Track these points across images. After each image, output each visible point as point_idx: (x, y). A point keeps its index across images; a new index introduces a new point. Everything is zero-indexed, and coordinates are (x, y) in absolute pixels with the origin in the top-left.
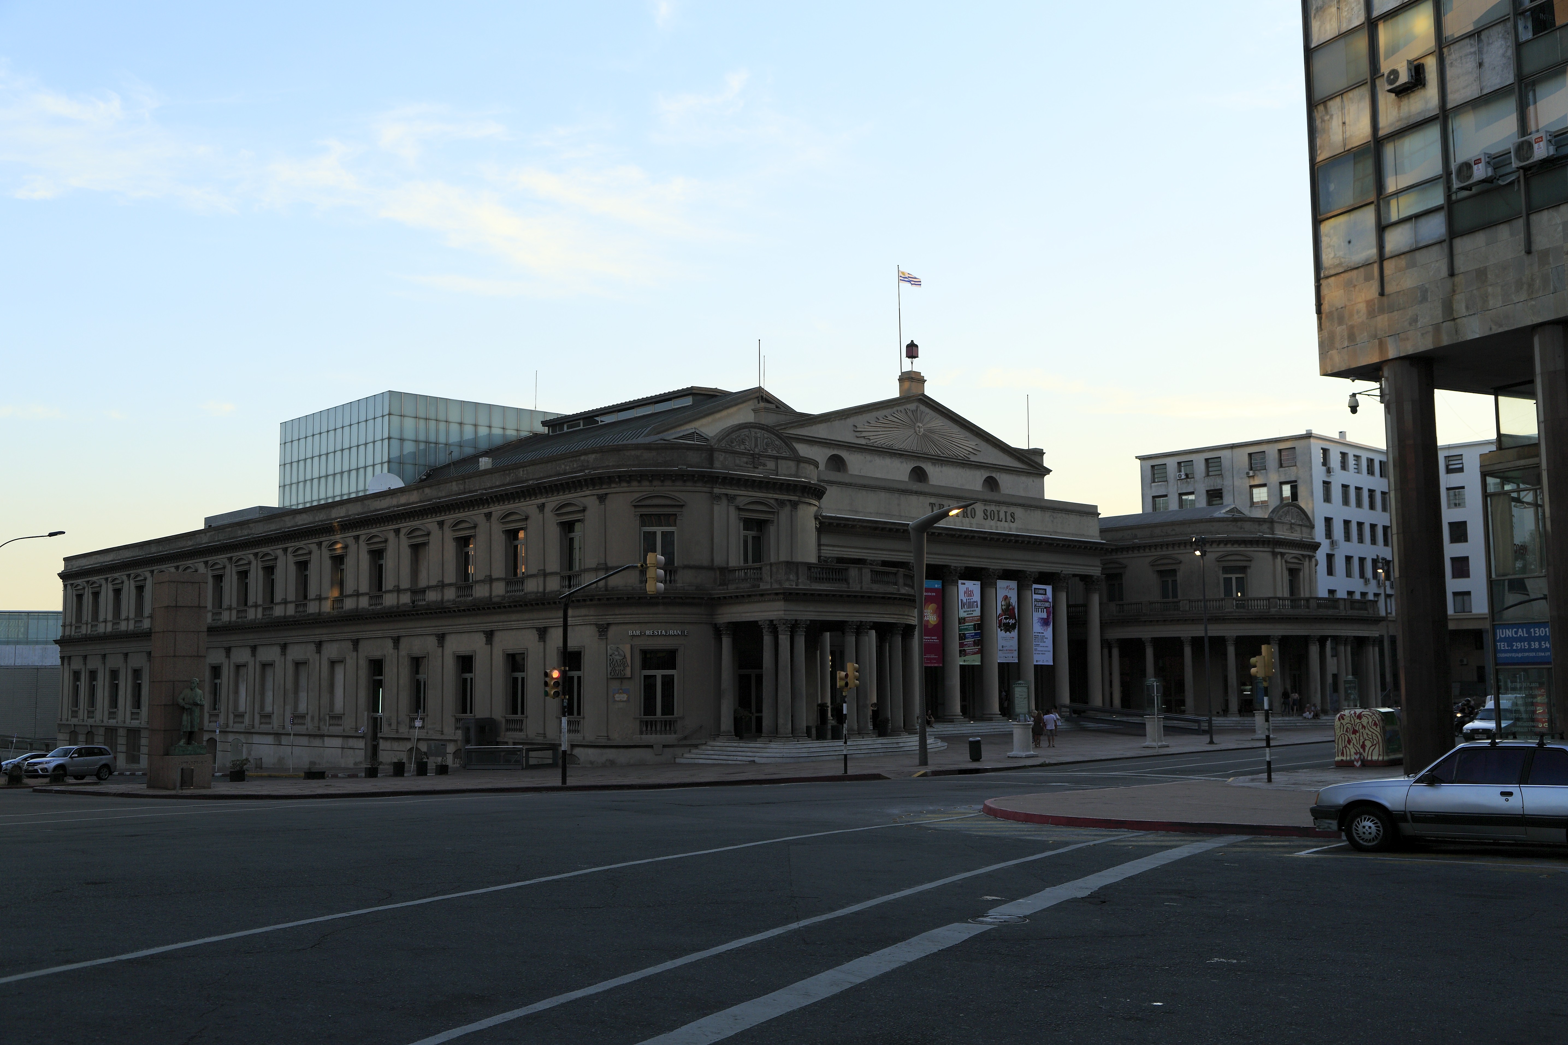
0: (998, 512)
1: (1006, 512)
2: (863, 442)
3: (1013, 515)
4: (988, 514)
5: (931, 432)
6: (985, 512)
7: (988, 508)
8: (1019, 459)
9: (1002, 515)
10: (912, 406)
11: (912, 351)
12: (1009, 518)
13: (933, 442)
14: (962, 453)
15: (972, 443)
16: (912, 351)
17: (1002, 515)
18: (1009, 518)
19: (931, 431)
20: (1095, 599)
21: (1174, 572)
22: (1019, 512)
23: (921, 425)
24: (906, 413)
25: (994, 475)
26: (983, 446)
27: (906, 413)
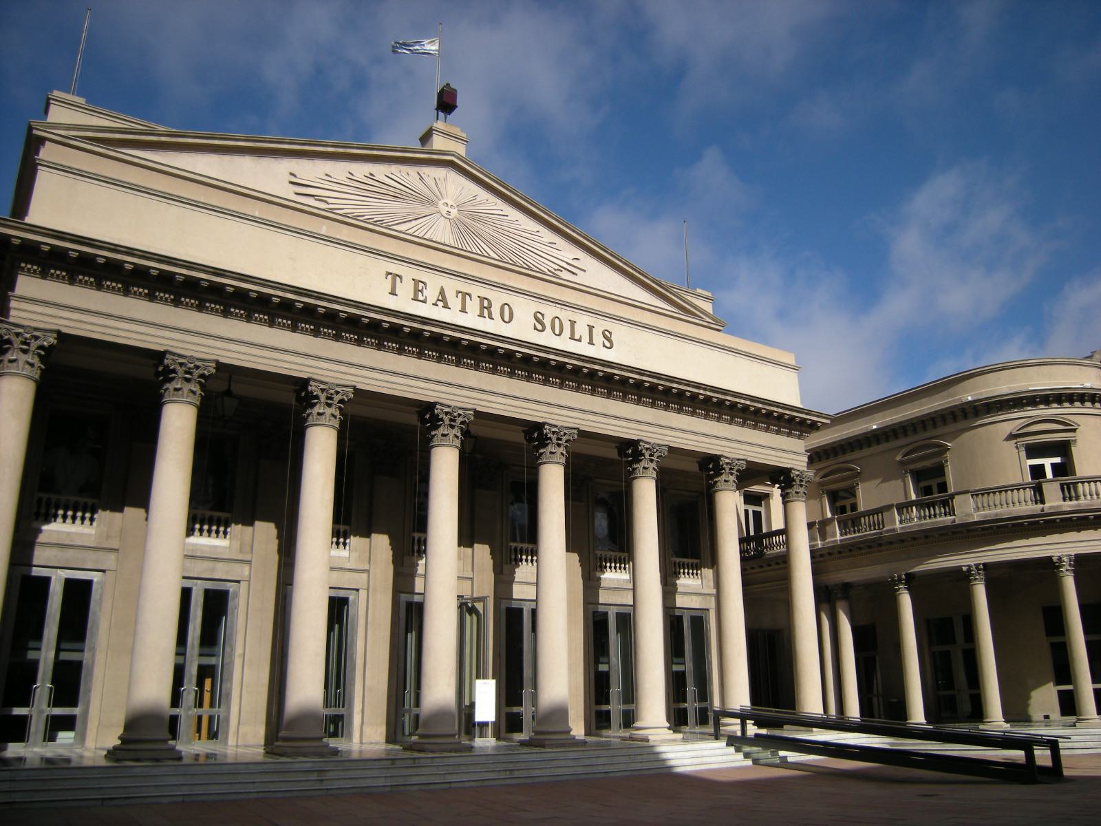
0: (573, 323)
1: (591, 328)
3: (607, 336)
5: (477, 220)
6: (538, 319)
9: (582, 330)
10: (440, 172)
12: (599, 338)
13: (480, 236)
17: (582, 330)
19: (476, 217)
20: (801, 513)
21: (940, 470)
22: (620, 332)
23: (450, 203)
24: (421, 178)
26: (587, 261)
27: (421, 178)
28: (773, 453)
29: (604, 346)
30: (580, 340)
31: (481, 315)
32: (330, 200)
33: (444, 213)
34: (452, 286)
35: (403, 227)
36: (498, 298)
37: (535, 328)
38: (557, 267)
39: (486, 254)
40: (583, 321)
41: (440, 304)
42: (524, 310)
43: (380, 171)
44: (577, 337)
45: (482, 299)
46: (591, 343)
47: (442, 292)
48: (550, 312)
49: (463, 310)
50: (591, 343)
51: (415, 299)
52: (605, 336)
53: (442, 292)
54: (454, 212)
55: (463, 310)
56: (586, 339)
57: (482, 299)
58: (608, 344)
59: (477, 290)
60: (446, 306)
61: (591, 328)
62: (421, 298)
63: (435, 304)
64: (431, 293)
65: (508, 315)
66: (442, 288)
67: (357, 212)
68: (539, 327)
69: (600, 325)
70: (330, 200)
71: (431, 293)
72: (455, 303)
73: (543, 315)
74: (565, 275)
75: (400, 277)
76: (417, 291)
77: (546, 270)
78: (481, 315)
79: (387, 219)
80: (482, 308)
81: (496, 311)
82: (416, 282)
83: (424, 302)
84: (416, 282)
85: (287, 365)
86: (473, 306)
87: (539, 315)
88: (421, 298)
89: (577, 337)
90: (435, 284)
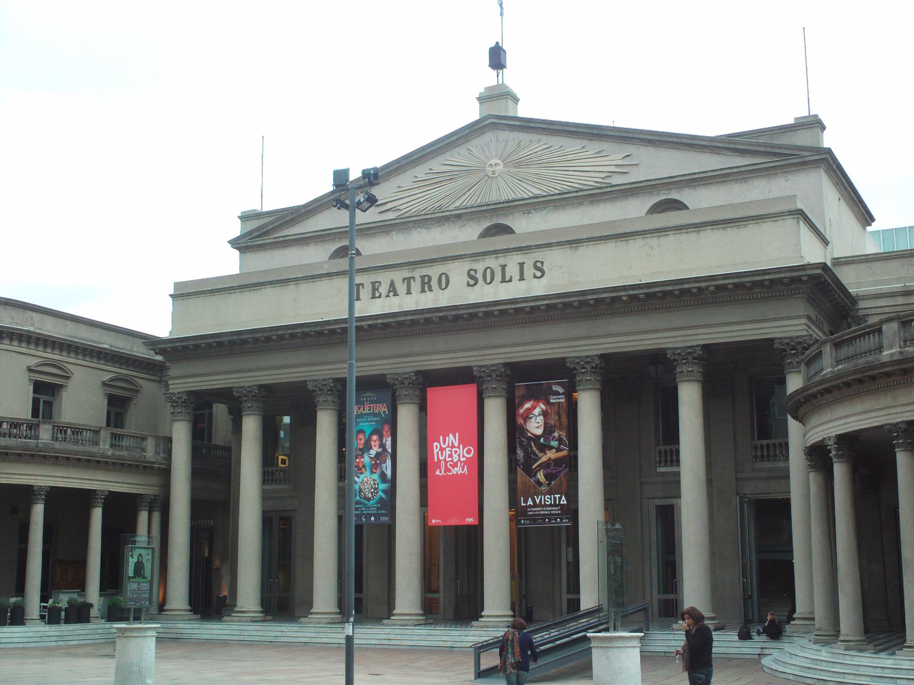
0: (503, 267)
1: (521, 265)
2: (390, 216)
4: (479, 276)
7: (475, 266)
8: (743, 152)
9: (512, 270)
11: (497, 58)
12: (529, 271)
14: (590, 180)
15: (616, 155)
16: (497, 58)
17: (512, 270)
18: (529, 271)
19: (519, 164)
23: (493, 161)
25: (675, 195)
28: (748, 326)
29: (535, 277)
30: (510, 281)
31: (423, 291)
32: (401, 207)
33: (490, 174)
34: (398, 276)
35: (457, 204)
36: (434, 272)
37: (469, 285)
38: (603, 175)
39: (531, 195)
40: (512, 263)
41: (391, 294)
42: (458, 272)
43: (436, 165)
44: (507, 279)
45: (423, 277)
46: (522, 278)
47: (392, 284)
48: (480, 266)
49: (409, 292)
50: (522, 278)
51: (373, 297)
52: (536, 268)
53: (392, 284)
54: (500, 168)
55: (409, 292)
56: (516, 276)
57: (423, 277)
58: (539, 274)
59: (419, 273)
60: (396, 294)
61: (521, 265)
62: (377, 295)
63: (388, 296)
64: (384, 289)
65: (445, 282)
66: (392, 282)
67: (422, 207)
68: (472, 282)
69: (529, 260)
70: (401, 207)
71: (384, 289)
72: (401, 288)
73: (476, 271)
74: (616, 180)
75: (362, 285)
76: (374, 290)
77: (593, 184)
78: (423, 291)
79: (444, 202)
80: (423, 284)
81: (434, 283)
82: (373, 283)
83: (380, 297)
84: (373, 283)
85: (296, 375)
86: (416, 286)
87: (472, 273)
88: (377, 295)
89: (507, 279)
90: (384, 278)
